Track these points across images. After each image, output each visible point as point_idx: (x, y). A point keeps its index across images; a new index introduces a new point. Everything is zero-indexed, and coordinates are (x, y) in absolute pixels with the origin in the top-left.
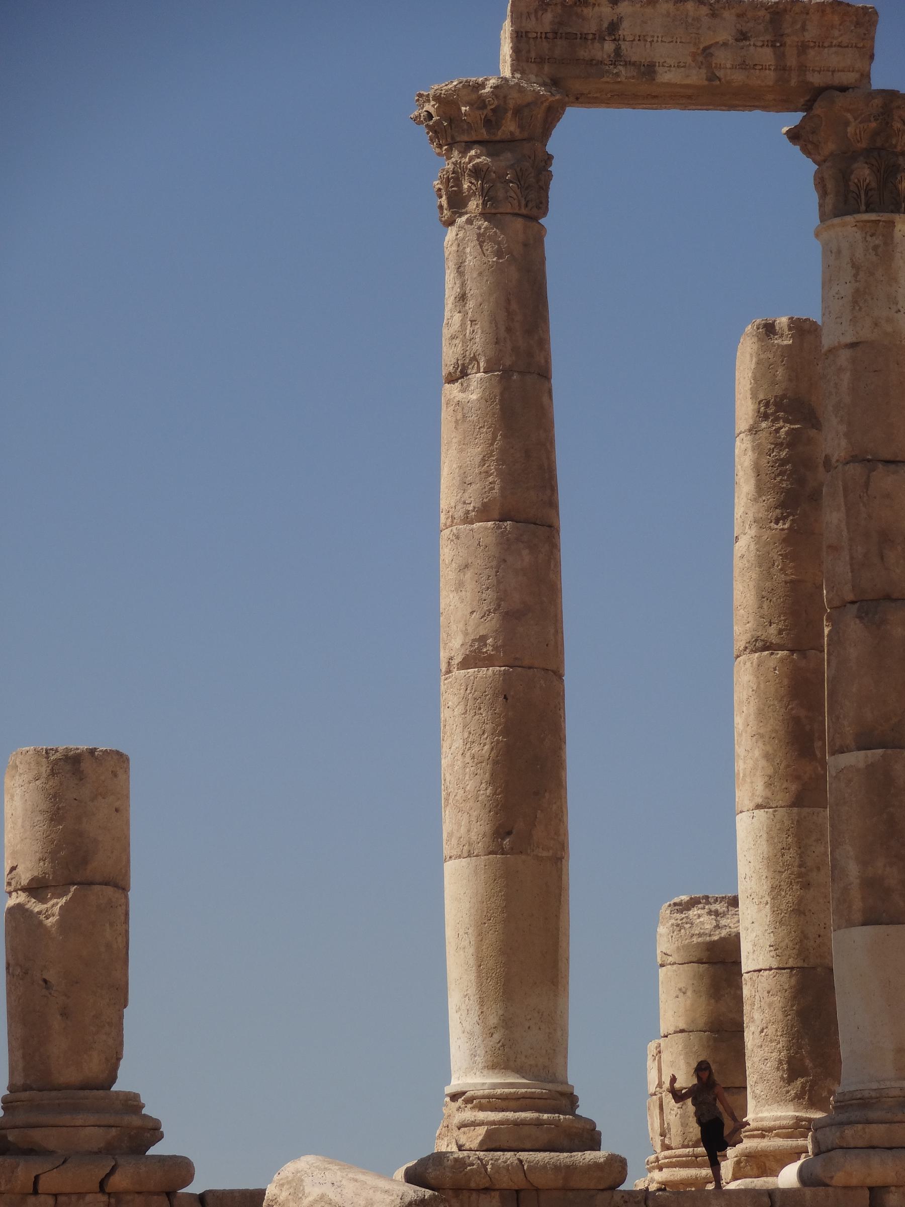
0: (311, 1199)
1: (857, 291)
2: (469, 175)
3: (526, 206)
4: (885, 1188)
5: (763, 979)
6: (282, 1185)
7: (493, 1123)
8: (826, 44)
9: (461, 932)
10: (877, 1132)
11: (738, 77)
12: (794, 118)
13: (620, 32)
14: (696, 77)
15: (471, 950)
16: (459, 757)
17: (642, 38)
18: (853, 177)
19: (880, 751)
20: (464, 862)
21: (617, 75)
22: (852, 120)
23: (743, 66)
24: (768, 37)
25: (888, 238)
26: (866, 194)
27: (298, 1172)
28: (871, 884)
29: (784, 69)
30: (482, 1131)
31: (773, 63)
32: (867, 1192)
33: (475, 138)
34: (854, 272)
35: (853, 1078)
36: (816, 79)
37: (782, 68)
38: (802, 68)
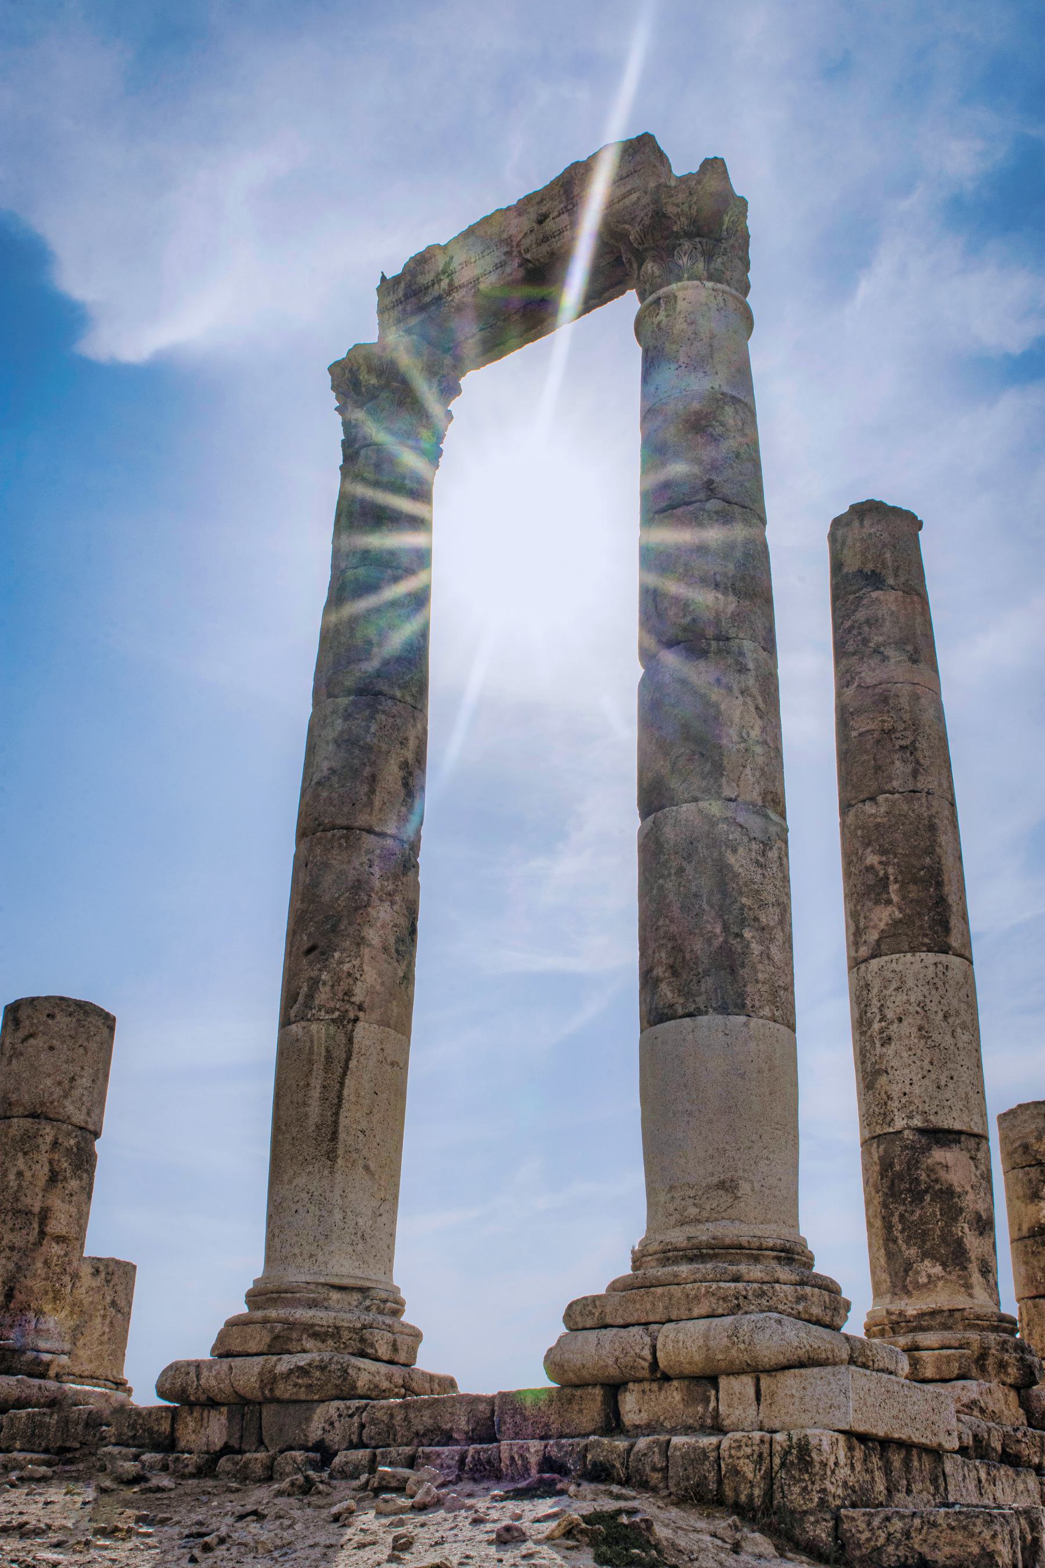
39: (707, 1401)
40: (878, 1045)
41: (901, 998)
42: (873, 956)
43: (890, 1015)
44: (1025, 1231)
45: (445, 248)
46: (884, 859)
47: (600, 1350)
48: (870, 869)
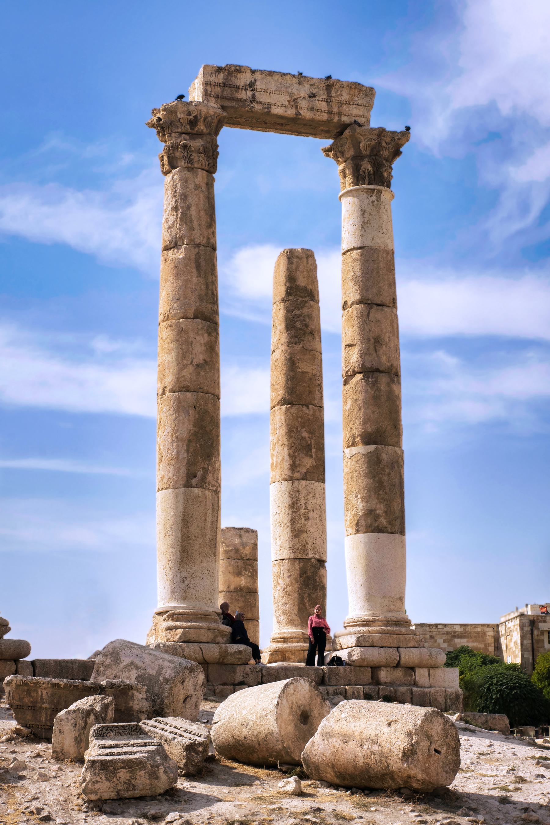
0: (125, 664)
1: (364, 222)
2: (180, 148)
3: (208, 165)
5: (286, 564)
6: (106, 656)
7: (185, 628)
8: (351, 103)
9: (168, 527)
12: (331, 141)
13: (255, 87)
14: (291, 112)
15: (173, 537)
16: (169, 437)
17: (265, 91)
18: (362, 168)
19: (375, 446)
20: (170, 491)
21: (253, 107)
22: (363, 140)
23: (312, 109)
24: (325, 97)
26: (368, 177)
27: (115, 648)
29: (332, 113)
30: (180, 631)
31: (326, 109)
32: (370, 669)
33: (183, 131)
34: (362, 213)
37: (330, 112)
38: (340, 114)
39: (412, 676)
40: (303, 519)
41: (314, 501)
42: (303, 479)
43: (309, 507)
44: (232, 588)
45: (253, 72)
46: (310, 436)
47: (375, 655)
48: (303, 438)
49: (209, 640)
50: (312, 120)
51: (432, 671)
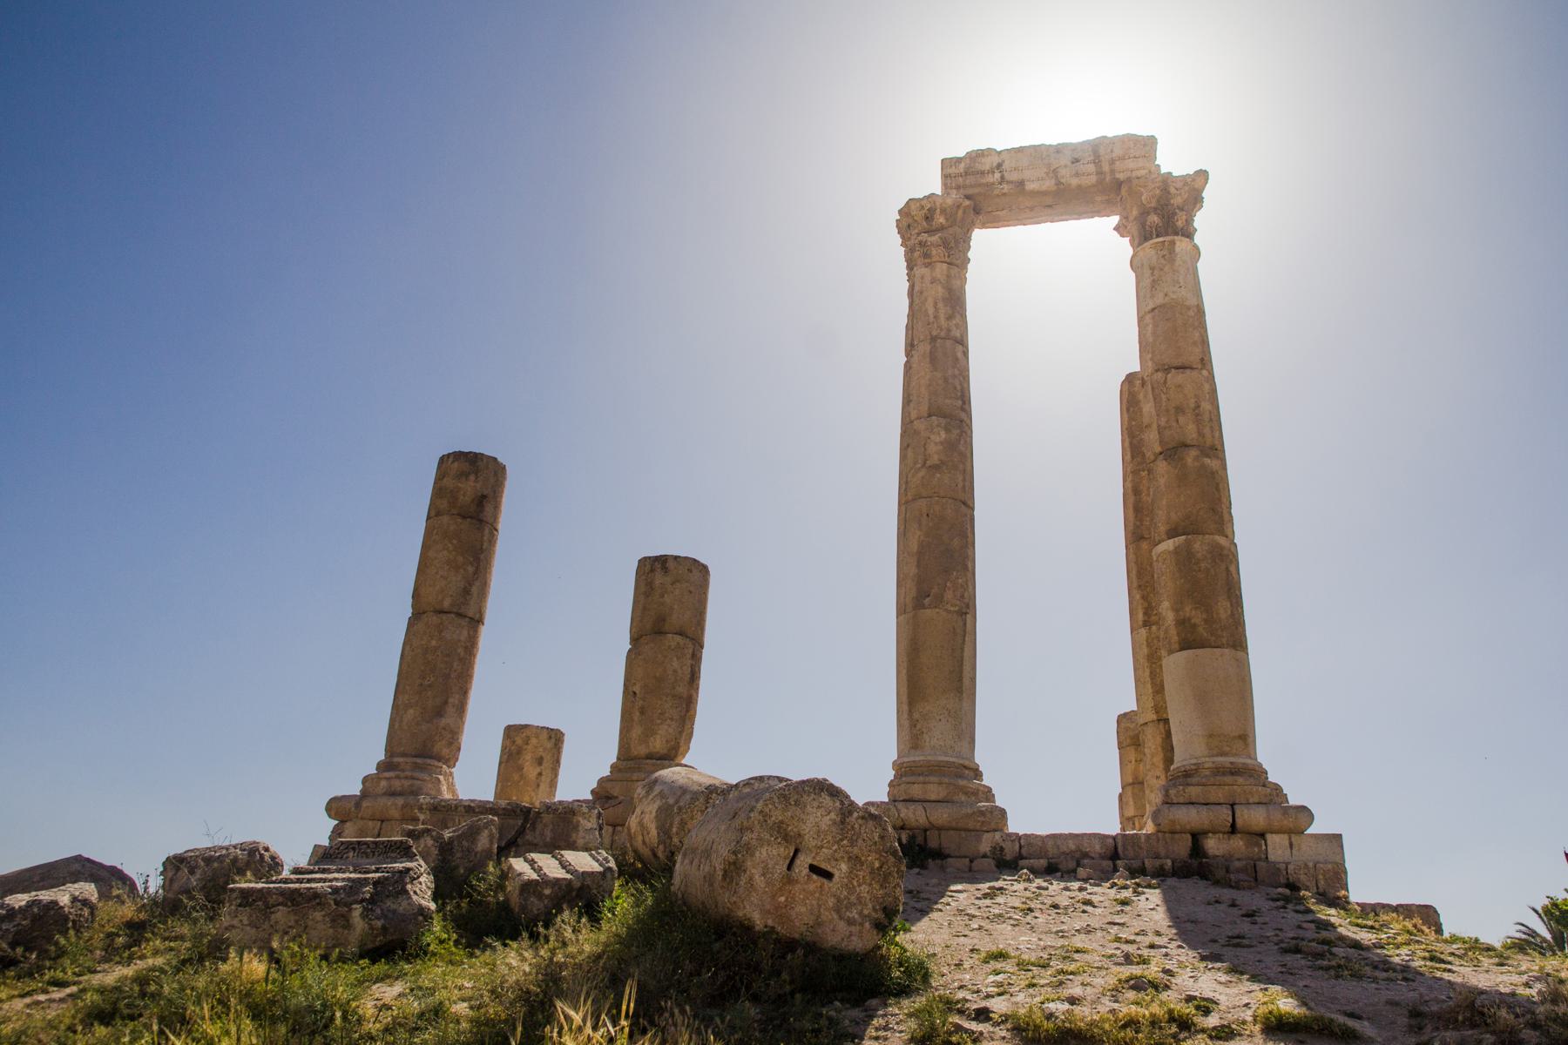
4: (1205, 833)
10: (1194, 792)
11: (1074, 182)
14: (1049, 184)
23: (1077, 175)
25: (1172, 251)
28: (1182, 623)
35: (1180, 759)
36: (1121, 176)
38: (1112, 172)
49: (940, 797)
50: (1079, 187)
51: (1294, 838)
